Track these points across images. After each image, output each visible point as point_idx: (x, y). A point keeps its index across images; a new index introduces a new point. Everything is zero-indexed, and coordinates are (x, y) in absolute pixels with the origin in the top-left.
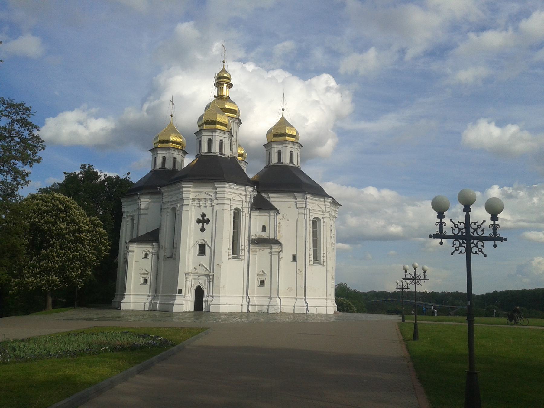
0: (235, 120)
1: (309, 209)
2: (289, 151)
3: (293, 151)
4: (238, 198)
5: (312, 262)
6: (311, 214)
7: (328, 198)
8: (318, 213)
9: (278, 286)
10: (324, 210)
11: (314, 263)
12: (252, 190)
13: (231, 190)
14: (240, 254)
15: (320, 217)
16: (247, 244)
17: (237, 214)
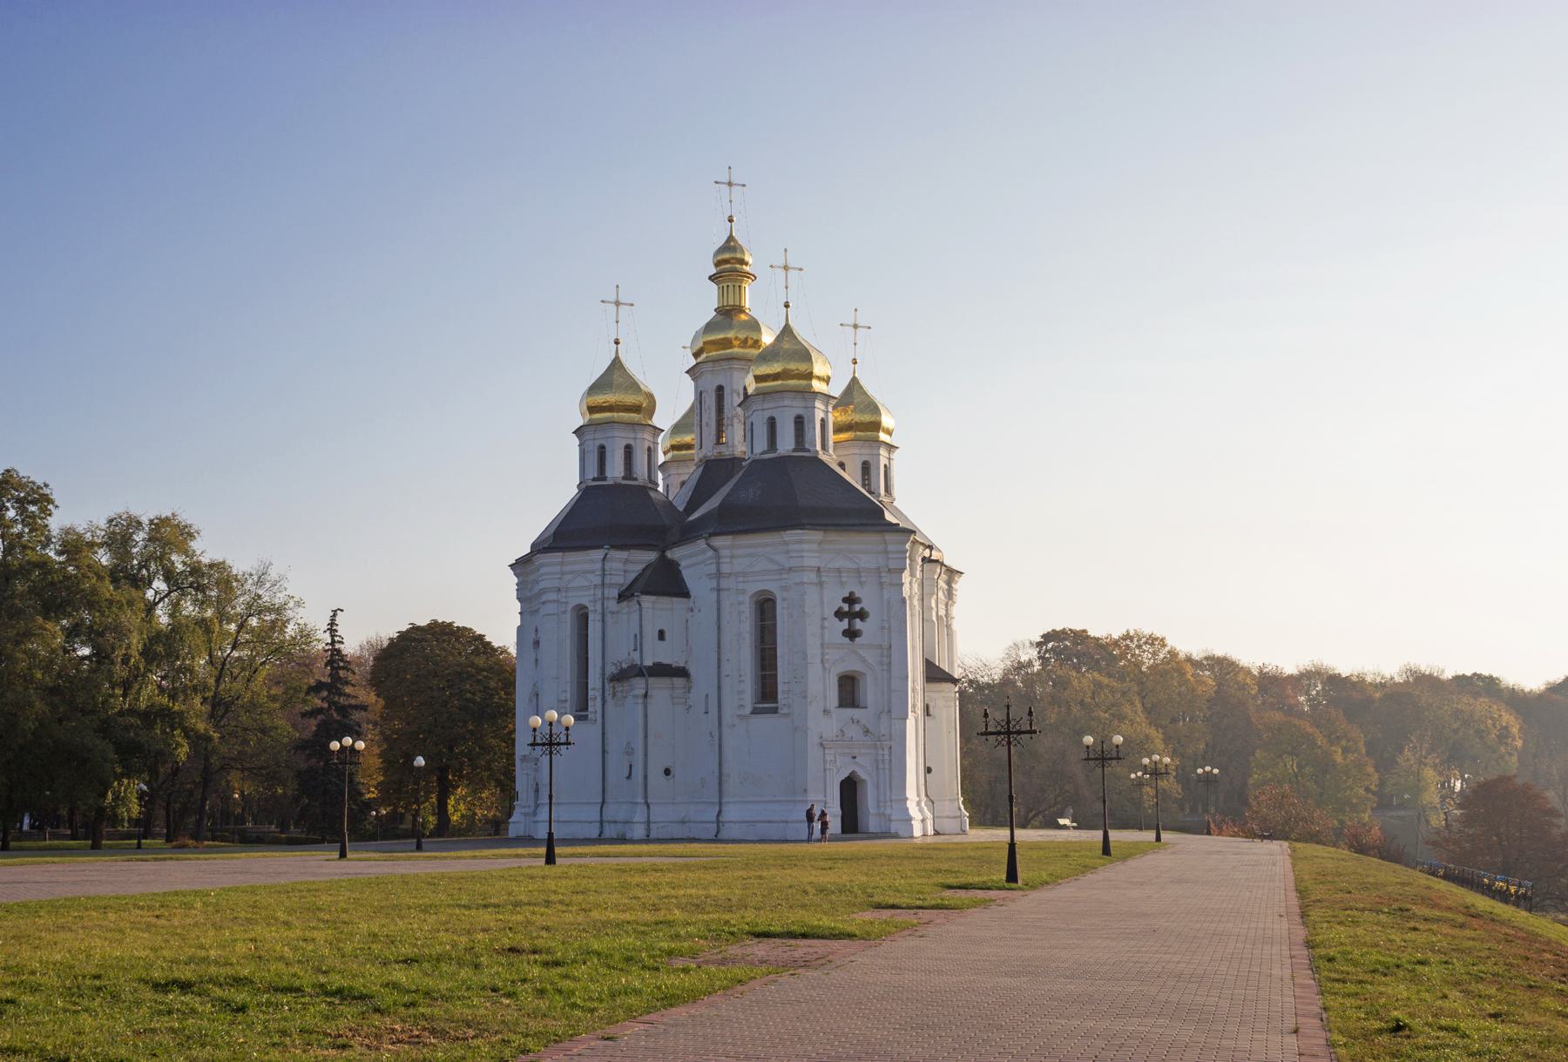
0: (726, 363)
1: (737, 574)
2: (765, 420)
3: (775, 413)
4: (580, 582)
5: (748, 709)
6: (741, 586)
7: (788, 532)
8: (766, 578)
9: (646, 777)
10: (787, 566)
11: (755, 712)
12: (602, 557)
13: (558, 569)
14: (590, 709)
15: (772, 587)
16: (599, 686)
17: (582, 616)
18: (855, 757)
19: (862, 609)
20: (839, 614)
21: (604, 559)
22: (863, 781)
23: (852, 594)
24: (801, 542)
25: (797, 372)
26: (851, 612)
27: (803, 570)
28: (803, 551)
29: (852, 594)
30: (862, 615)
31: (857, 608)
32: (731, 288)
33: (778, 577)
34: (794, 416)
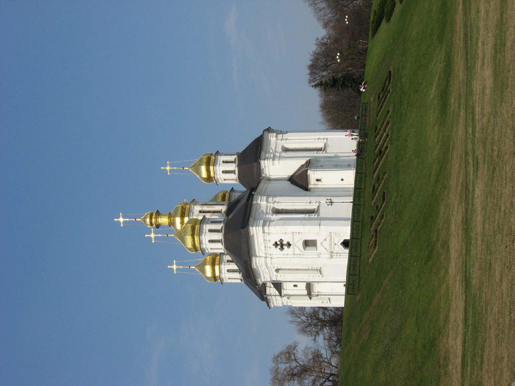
18: (335, 244)
19: (279, 241)
20: (282, 248)
21: (270, 296)
22: (344, 240)
23: (274, 245)
24: (256, 264)
25: (192, 242)
26: (280, 245)
27: (267, 263)
28: (259, 264)
29: (274, 245)
30: (281, 241)
31: (278, 243)
32: (161, 219)
33: (270, 269)
34: (209, 243)
